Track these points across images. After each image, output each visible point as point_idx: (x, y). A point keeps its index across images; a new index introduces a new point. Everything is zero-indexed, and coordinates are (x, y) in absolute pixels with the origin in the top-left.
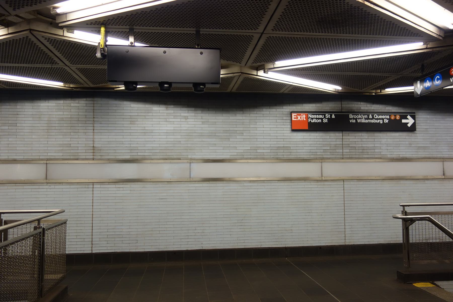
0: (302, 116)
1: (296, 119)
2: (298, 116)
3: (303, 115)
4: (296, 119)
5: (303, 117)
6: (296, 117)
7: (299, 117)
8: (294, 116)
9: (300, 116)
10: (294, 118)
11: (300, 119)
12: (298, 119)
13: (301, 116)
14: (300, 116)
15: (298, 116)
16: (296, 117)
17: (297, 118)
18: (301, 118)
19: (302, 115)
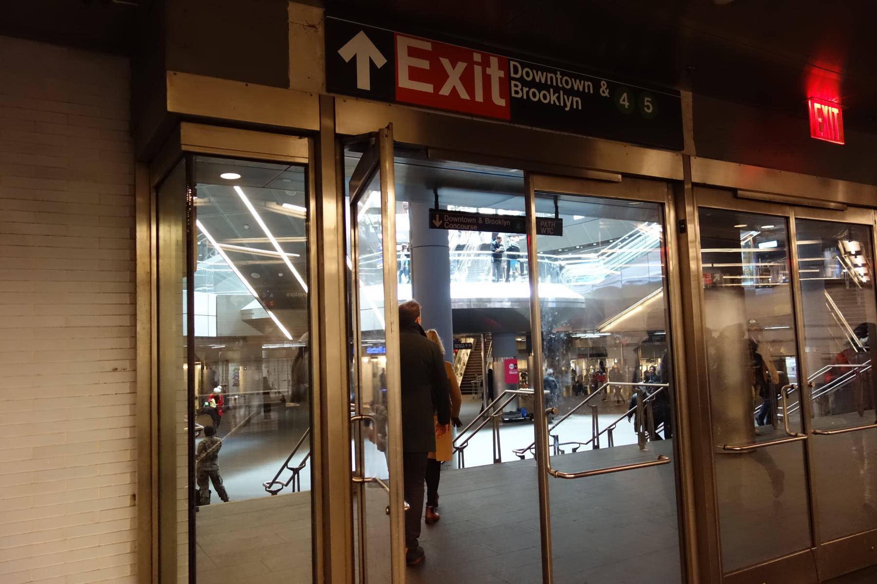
0: (478, 70)
1: (428, 88)
2: (445, 62)
3: (485, 64)
4: (428, 88)
5: (487, 79)
6: (425, 64)
7: (453, 83)
8: (413, 52)
9: (461, 66)
10: (415, 74)
11: (464, 95)
12: (445, 91)
13: (471, 64)
14: (461, 66)
15: (445, 62)
16: (425, 64)
17: (438, 77)
18: (467, 79)
19: (477, 57)
